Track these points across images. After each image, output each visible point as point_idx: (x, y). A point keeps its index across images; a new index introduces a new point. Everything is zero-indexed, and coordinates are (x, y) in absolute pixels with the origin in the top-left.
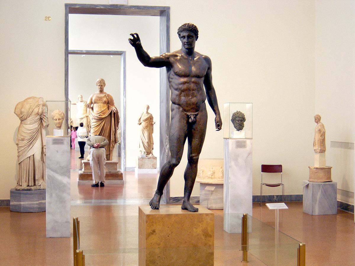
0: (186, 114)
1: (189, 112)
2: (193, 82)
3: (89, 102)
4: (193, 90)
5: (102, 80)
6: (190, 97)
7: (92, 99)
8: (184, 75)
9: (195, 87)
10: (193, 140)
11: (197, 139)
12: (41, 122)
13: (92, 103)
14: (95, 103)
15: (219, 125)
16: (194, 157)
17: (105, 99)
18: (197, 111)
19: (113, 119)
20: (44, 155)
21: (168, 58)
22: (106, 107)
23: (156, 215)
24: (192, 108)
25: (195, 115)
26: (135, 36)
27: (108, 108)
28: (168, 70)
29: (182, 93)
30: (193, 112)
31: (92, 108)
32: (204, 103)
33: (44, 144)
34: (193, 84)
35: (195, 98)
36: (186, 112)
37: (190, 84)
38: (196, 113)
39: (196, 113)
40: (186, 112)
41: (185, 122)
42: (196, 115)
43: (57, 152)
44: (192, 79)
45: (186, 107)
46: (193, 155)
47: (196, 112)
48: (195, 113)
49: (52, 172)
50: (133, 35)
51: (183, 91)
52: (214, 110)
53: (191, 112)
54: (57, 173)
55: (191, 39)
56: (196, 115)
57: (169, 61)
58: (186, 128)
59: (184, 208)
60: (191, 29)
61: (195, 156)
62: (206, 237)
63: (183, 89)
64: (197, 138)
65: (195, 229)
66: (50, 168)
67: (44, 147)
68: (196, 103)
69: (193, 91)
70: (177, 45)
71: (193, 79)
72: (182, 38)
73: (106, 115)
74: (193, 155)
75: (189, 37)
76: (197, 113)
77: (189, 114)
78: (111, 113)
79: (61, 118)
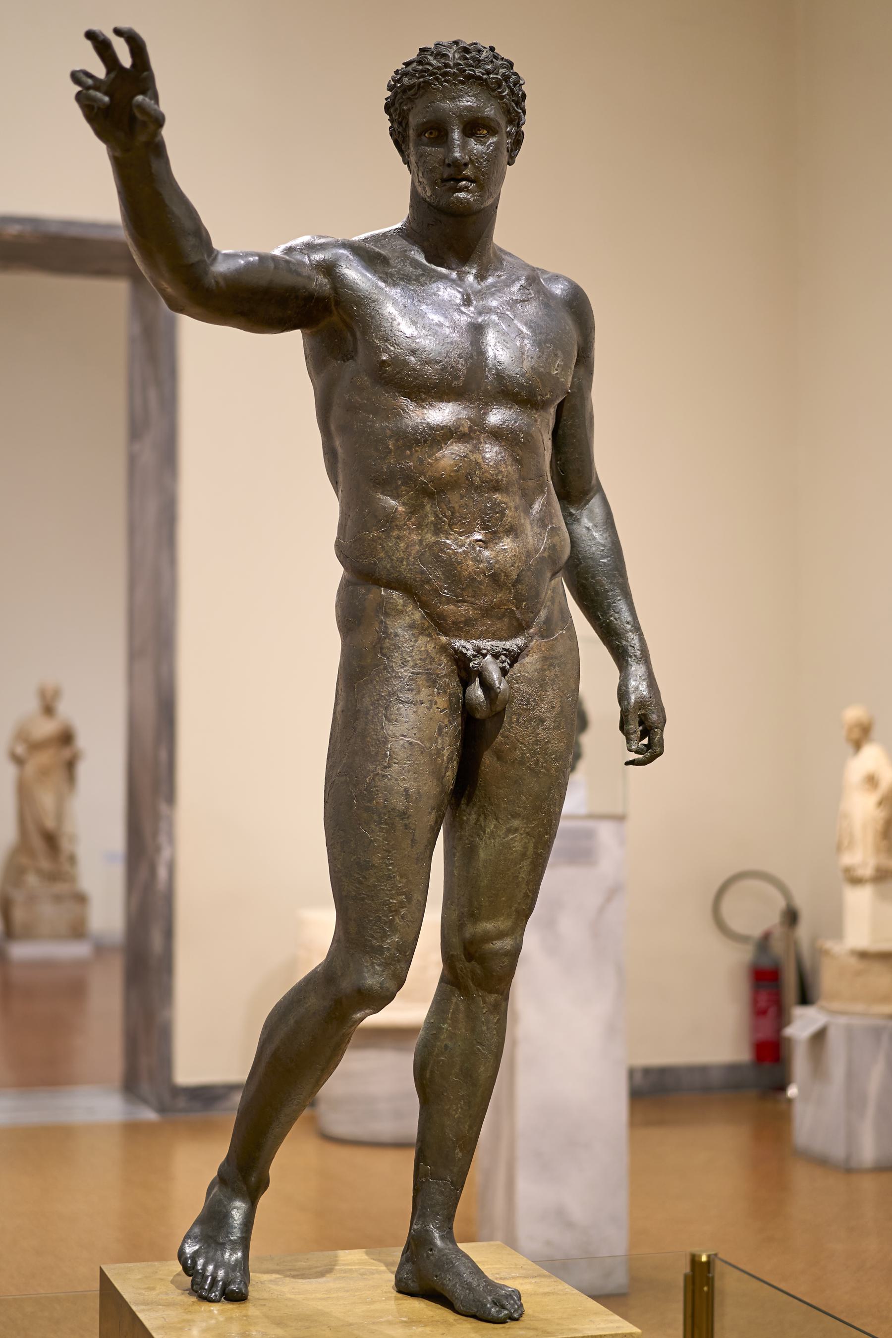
0: (444, 649)
1: (468, 637)
2: (497, 434)
4: (496, 487)
6: (478, 536)
8: (436, 385)
9: (509, 470)
10: (491, 826)
11: (516, 823)
15: (644, 728)
16: (488, 938)
18: (519, 628)
21: (329, 269)
24: (486, 612)
26: (125, 59)
29: (422, 506)
30: (494, 637)
34: (496, 449)
35: (507, 544)
36: (446, 634)
37: (476, 449)
38: (513, 644)
39: (513, 644)
40: (444, 639)
41: (442, 702)
42: (514, 657)
46: (488, 926)
47: (513, 636)
48: (508, 644)
50: (102, 47)
51: (431, 495)
52: (610, 636)
53: (479, 638)
55: (481, 140)
56: (514, 657)
58: (447, 747)
59: (413, 1286)
60: (488, 73)
61: (501, 935)
64: (515, 815)
69: (497, 496)
70: (380, 195)
71: (496, 417)
74: (488, 926)
75: (474, 126)
77: (467, 646)
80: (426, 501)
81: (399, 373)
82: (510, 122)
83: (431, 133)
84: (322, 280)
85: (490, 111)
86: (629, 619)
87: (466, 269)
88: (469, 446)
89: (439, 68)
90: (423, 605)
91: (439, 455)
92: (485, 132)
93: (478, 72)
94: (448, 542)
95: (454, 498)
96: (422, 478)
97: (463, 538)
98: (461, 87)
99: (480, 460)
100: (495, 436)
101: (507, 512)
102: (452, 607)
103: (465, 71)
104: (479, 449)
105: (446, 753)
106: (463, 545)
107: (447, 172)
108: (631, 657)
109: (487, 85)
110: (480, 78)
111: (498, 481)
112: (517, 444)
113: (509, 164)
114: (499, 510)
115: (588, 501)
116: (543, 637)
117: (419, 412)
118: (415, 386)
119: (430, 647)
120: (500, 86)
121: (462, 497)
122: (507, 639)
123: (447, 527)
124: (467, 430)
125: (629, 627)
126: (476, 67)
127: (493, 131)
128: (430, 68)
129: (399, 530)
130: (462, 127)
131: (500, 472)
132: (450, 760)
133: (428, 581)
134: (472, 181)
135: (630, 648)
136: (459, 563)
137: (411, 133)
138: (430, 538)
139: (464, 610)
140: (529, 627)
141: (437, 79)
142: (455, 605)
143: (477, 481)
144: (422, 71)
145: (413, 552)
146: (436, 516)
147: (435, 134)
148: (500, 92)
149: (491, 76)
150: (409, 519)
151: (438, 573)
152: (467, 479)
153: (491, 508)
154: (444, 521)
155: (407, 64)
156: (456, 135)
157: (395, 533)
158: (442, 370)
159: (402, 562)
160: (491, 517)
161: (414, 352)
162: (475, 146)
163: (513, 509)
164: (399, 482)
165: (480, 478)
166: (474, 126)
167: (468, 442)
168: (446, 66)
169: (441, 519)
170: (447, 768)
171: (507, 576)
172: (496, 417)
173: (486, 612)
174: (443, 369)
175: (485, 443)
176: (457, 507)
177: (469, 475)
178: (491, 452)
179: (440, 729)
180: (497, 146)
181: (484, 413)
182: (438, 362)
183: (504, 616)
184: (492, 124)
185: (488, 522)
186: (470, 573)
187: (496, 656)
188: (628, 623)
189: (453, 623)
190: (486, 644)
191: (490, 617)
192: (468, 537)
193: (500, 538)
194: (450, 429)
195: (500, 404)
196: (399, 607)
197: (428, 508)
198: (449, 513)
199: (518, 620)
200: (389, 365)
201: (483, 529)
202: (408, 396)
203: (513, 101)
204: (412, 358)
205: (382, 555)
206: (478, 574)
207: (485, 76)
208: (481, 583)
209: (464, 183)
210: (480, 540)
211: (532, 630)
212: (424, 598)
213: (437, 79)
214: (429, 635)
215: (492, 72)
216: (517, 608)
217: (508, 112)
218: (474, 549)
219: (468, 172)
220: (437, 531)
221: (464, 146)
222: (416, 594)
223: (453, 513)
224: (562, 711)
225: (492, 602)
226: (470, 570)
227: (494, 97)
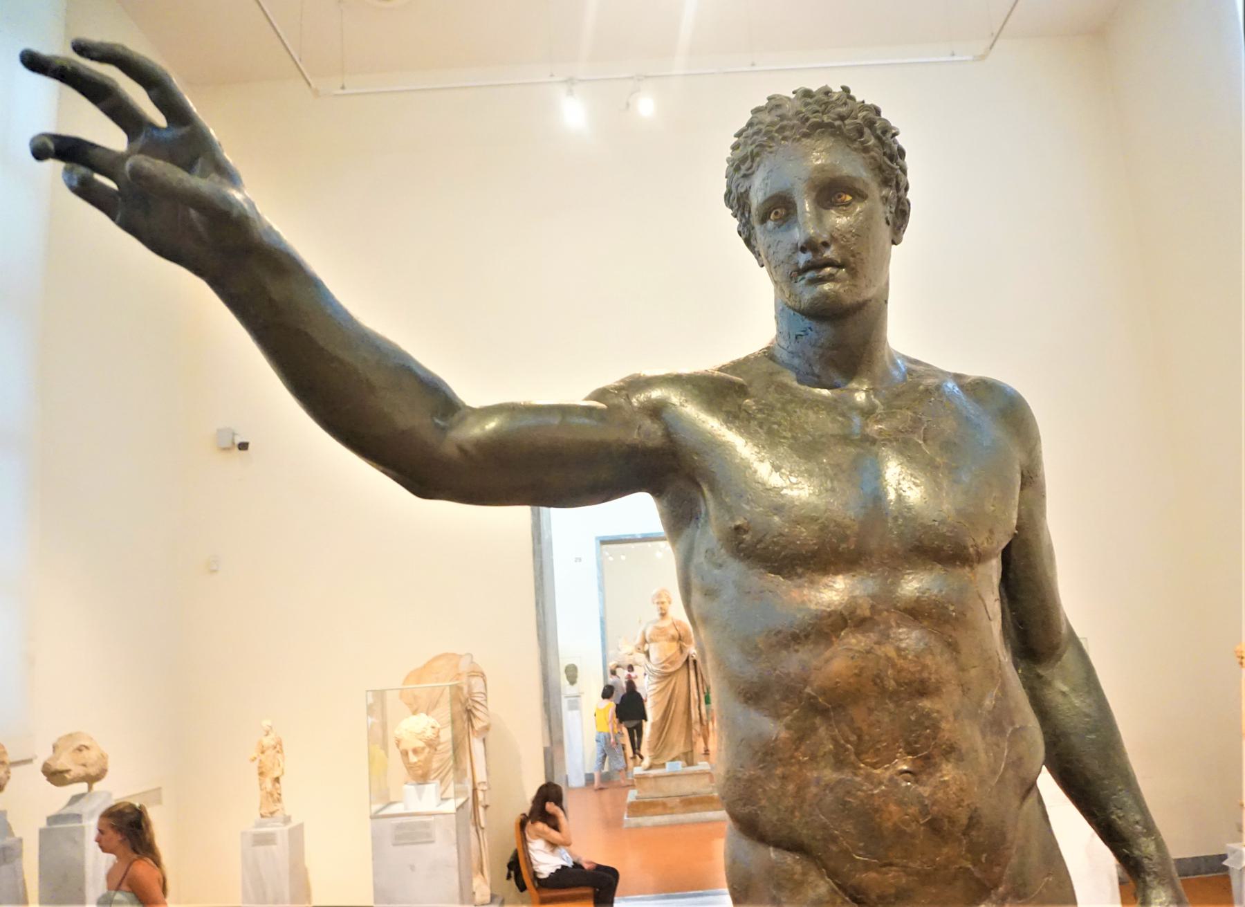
2: (915, 612)
3: (639, 640)
5: (664, 590)
6: (905, 767)
7: (644, 633)
12: (470, 720)
13: (645, 642)
14: (652, 641)
17: (673, 632)
19: (692, 673)
20: (481, 809)
22: (675, 646)
24: (926, 878)
27: (681, 649)
28: (681, 518)
29: (814, 729)
31: (647, 654)
32: (1031, 800)
33: (478, 780)
34: (915, 634)
35: (948, 771)
37: (885, 637)
43: (412, 868)
44: (896, 584)
45: (867, 867)
51: (823, 712)
57: (668, 434)
60: (842, 118)
63: (823, 691)
67: (480, 788)
68: (964, 820)
69: (926, 704)
72: (770, 224)
73: (678, 666)
75: (831, 192)
78: (687, 661)
79: (421, 744)
80: (818, 721)
81: (760, 541)
82: (885, 182)
83: (776, 213)
84: (648, 424)
85: (853, 166)
86: (1138, 817)
87: (854, 385)
88: (873, 636)
89: (772, 124)
90: (833, 874)
91: (828, 654)
92: (849, 198)
93: (826, 119)
94: (858, 779)
95: (858, 714)
96: (808, 690)
97: (878, 771)
98: (806, 141)
99: (892, 654)
100: (911, 614)
101: (943, 725)
102: (873, 875)
103: (807, 119)
104: (888, 636)
106: (881, 783)
107: (803, 258)
108: (1149, 874)
109: (842, 134)
110: (830, 125)
111: (922, 681)
112: (947, 622)
113: (894, 243)
114: (929, 723)
115: (1061, 656)
117: (795, 594)
118: (785, 557)
120: (861, 134)
121: (871, 711)
123: (853, 757)
124: (867, 613)
125: (1139, 828)
126: (823, 113)
127: (860, 195)
128: (761, 126)
129: (784, 766)
130: (814, 194)
131: (925, 667)
133: (834, 839)
134: (839, 266)
135: (1146, 861)
136: (877, 811)
137: (755, 220)
138: (829, 775)
139: (894, 877)
140: (996, 886)
141: (772, 138)
142: (877, 872)
143: (891, 685)
144: (755, 134)
145: (809, 796)
146: (834, 740)
147: (782, 212)
148: (862, 143)
149: (847, 122)
150: (797, 749)
151: (849, 827)
152: (876, 684)
153: (917, 722)
154: (847, 750)
155: (738, 135)
156: (806, 206)
157: (779, 771)
158: (821, 530)
159: (792, 812)
160: (919, 736)
161: (778, 509)
162: (839, 220)
163: (951, 719)
164: (777, 697)
165: (896, 681)
166: (831, 192)
167: (871, 630)
168: (782, 117)
169: (843, 746)
171: (952, 821)
172: (913, 585)
173: (926, 878)
174: (824, 528)
175: (899, 626)
176: (865, 728)
177: (878, 679)
178: (910, 638)
180: (869, 216)
181: (893, 583)
182: (814, 520)
183: (955, 877)
184: (859, 186)
185: (916, 743)
186: (895, 824)
188: (1137, 823)
189: (879, 897)
192: (887, 769)
193: (936, 767)
194: (841, 614)
195: (914, 567)
196: (796, 877)
197: (822, 731)
198: (854, 738)
199: (978, 881)
200: (746, 532)
201: (909, 754)
202: (777, 571)
203: (885, 154)
204: (776, 519)
205: (763, 802)
207: (837, 123)
208: (913, 836)
209: (828, 269)
210: (906, 772)
211: (1001, 889)
212: (831, 864)
213: (772, 138)
215: (848, 117)
216: (975, 865)
217: (879, 169)
218: (897, 785)
219: (829, 253)
220: (840, 762)
221: (819, 219)
222: (819, 858)
223: (860, 737)
225: (933, 861)
226: (896, 818)
227: (855, 150)
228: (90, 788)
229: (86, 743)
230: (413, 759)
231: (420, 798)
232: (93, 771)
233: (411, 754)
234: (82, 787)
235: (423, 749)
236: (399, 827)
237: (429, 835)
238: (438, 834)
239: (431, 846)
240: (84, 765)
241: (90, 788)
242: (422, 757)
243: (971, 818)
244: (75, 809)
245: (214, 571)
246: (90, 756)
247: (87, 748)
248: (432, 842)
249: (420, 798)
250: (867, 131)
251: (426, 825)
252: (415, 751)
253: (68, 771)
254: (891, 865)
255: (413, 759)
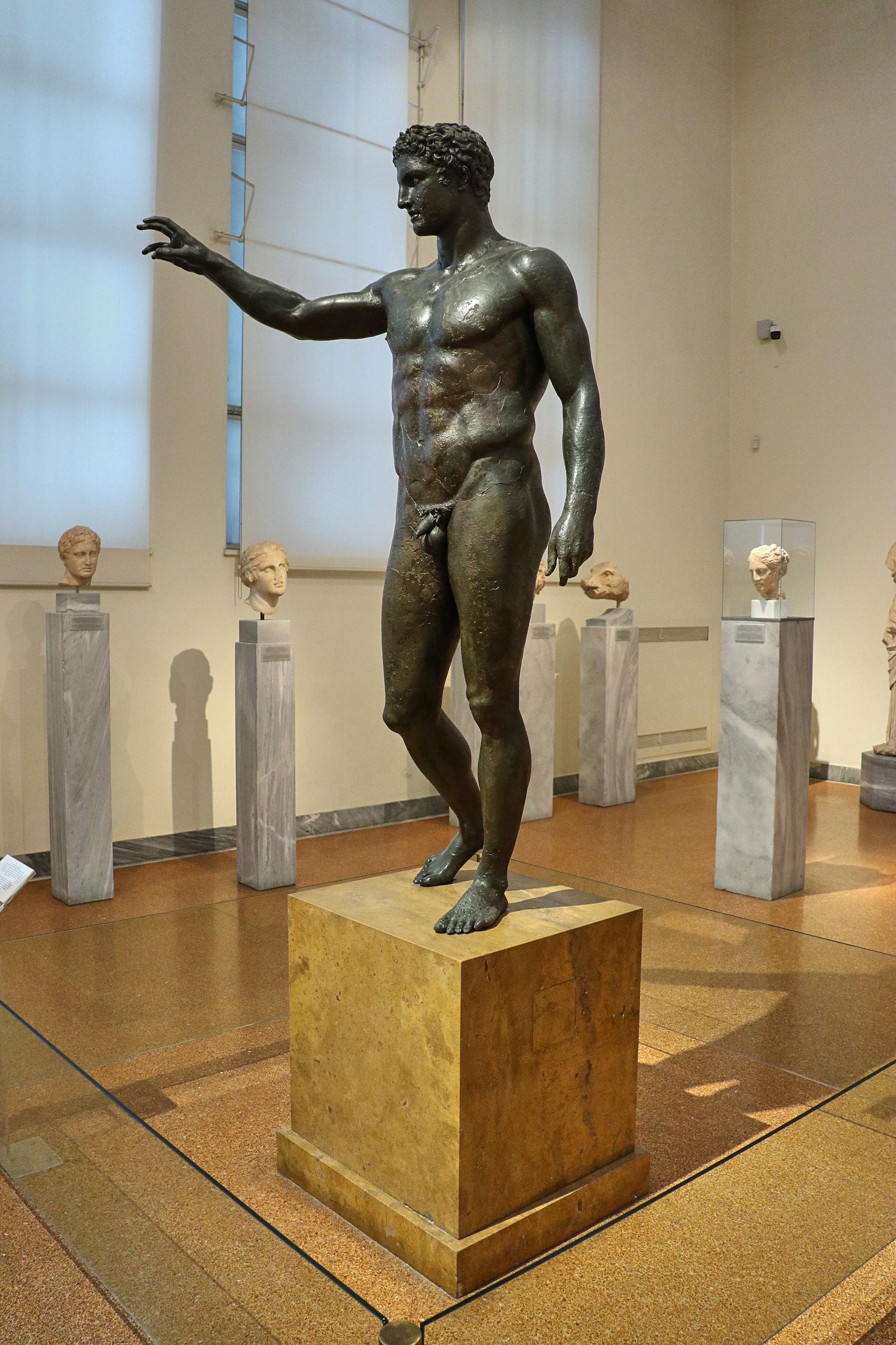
18: (448, 496)
23: (311, 906)
25: (440, 511)
38: (444, 506)
41: (416, 545)
43: (748, 661)
48: (438, 506)
49: (734, 716)
53: (428, 502)
54: (745, 719)
60: (409, 144)
62: (435, 1052)
65: (403, 1005)
66: (729, 705)
76: (448, 504)
82: (438, 166)
92: (416, 180)
105: (419, 577)
116: (464, 499)
119: (411, 510)
122: (442, 502)
132: (423, 581)
134: (418, 213)
170: (422, 587)
179: (414, 562)
187: (433, 513)
190: (428, 507)
191: (429, 489)
206: (419, 462)
214: (411, 504)
217: (430, 160)
224: (472, 548)
228: (618, 605)
229: (611, 570)
230: (757, 577)
231: (763, 611)
232: (616, 591)
233: (755, 573)
234: (612, 604)
235: (765, 570)
236: (741, 628)
237: (760, 637)
238: (767, 637)
239: (760, 645)
240: (609, 586)
241: (618, 605)
242: (764, 577)
243: (437, 460)
244: (603, 618)
245: (756, 450)
246: (614, 580)
247: (612, 574)
248: (762, 642)
249: (763, 611)
250: (421, 146)
251: (759, 628)
252: (759, 572)
253: (596, 588)
254: (415, 481)
255: (757, 577)
